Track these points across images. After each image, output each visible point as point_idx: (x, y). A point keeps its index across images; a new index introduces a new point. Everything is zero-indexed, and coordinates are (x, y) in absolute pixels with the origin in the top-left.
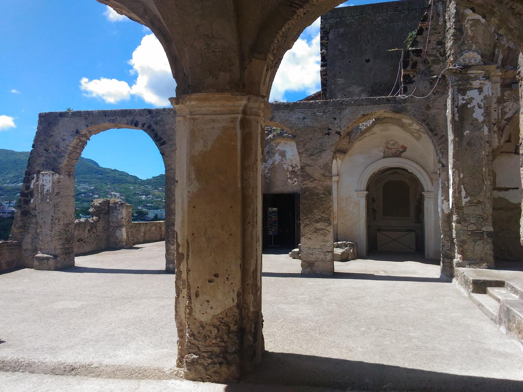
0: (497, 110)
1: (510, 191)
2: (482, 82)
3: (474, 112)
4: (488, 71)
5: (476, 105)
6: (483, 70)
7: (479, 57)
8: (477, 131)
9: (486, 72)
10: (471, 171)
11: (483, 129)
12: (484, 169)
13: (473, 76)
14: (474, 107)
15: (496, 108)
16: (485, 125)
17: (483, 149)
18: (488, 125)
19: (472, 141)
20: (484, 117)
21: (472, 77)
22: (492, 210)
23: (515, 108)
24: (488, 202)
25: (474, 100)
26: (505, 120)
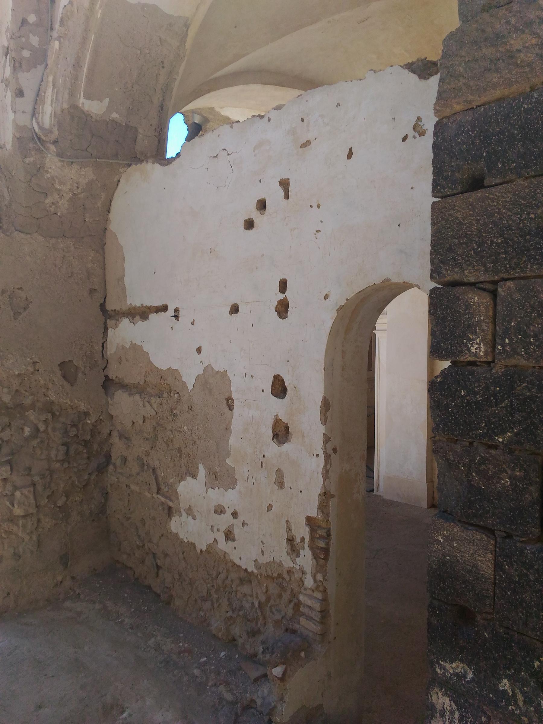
1: (153, 317)
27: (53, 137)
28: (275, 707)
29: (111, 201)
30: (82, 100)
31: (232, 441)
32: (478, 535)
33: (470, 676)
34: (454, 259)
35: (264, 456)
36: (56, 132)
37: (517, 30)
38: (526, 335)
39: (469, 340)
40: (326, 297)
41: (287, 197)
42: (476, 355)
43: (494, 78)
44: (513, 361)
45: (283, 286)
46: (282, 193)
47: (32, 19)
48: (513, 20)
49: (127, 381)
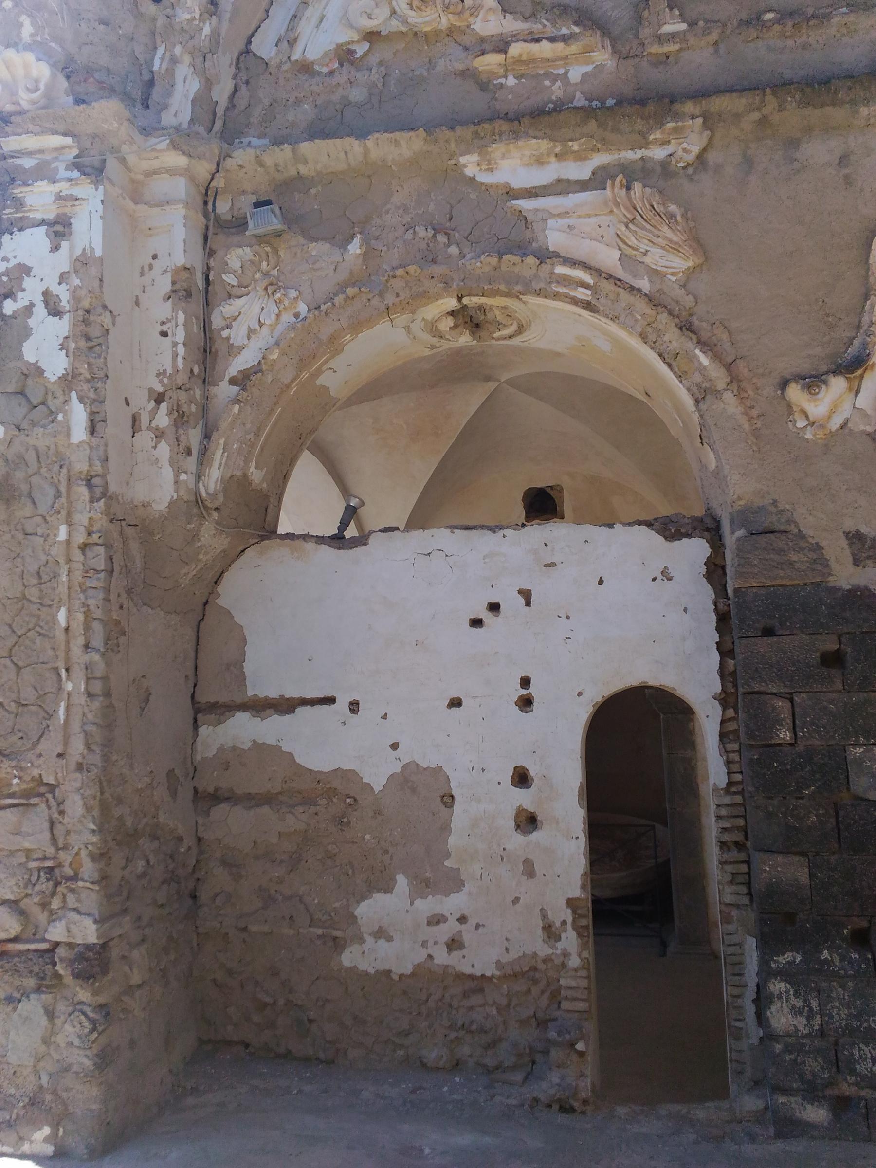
0: (170, 334)
1: (300, 710)
2: (63, 187)
3: (27, 333)
4: (95, 136)
5: (39, 300)
6: (65, 134)
7: (43, 71)
8: (44, 427)
9: (88, 144)
10: (10, 626)
11: (65, 413)
12: (62, 616)
13: (28, 163)
14: (29, 309)
15: (169, 321)
16: (74, 394)
17: (64, 513)
18: (92, 395)
19: (19, 475)
20: (75, 355)
21: (25, 171)
22: (92, 827)
23: (268, 322)
24: (79, 785)
25: (28, 275)
26: (233, 381)
27: (217, 504)
28: (577, 1085)
29: (222, 573)
30: (252, 469)
31: (452, 841)
32: (797, 859)
33: (799, 959)
34: (760, 677)
35: (504, 849)
36: (221, 498)
37: (794, 550)
38: (818, 726)
39: (777, 730)
40: (580, 694)
41: (528, 604)
42: (784, 739)
43: (782, 573)
44: (809, 742)
45: (525, 682)
46: (523, 601)
47: (196, 370)
48: (791, 544)
49: (239, 791)
